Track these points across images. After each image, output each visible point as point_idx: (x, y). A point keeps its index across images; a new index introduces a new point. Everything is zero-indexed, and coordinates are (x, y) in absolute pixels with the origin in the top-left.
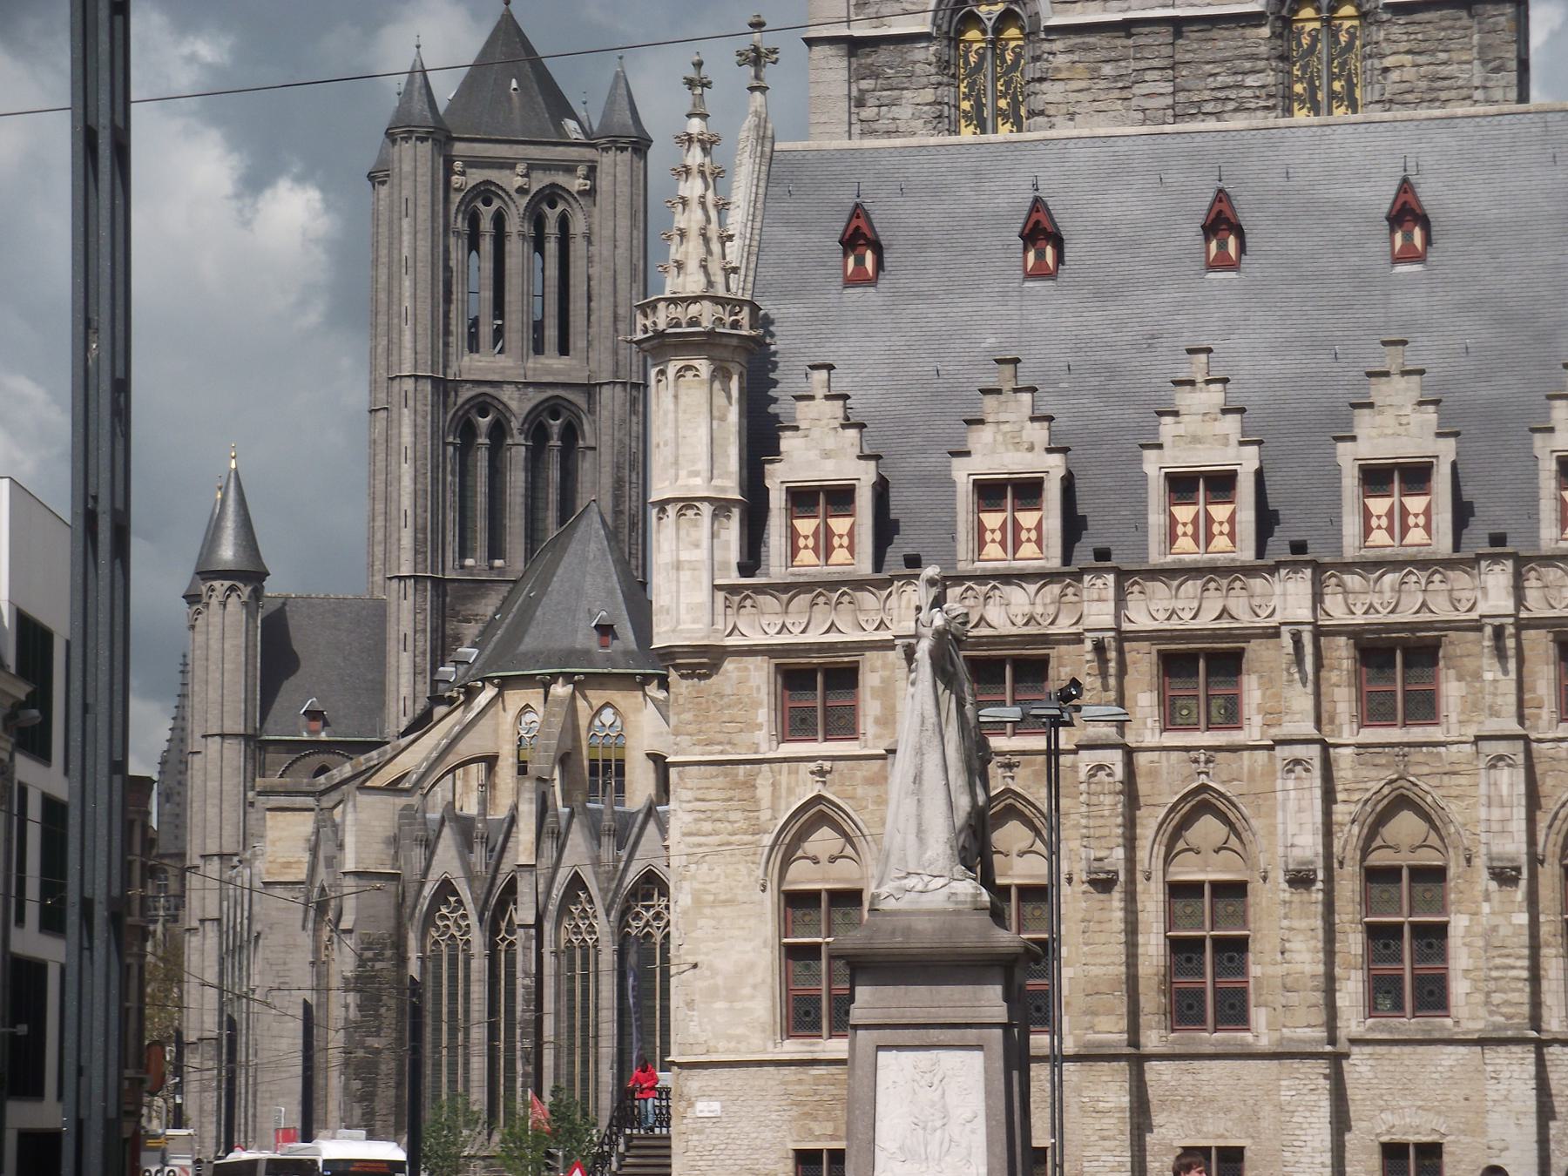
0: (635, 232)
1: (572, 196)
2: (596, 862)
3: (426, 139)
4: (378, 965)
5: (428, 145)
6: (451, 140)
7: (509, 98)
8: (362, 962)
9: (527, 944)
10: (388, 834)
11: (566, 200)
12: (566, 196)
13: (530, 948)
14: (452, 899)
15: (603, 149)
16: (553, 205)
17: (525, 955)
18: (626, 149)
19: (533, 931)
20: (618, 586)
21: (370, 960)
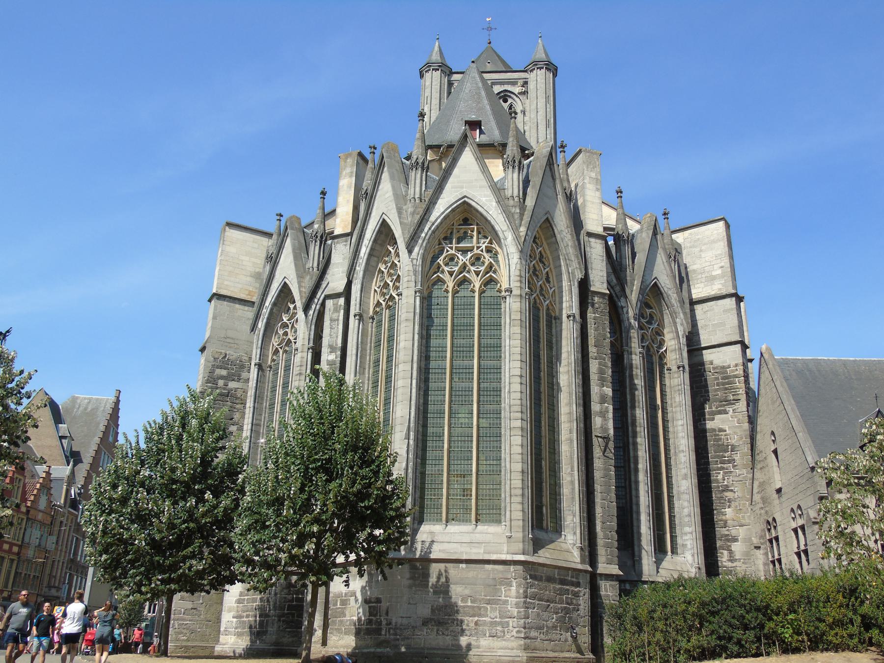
0: (548, 105)
1: (515, 95)
2: (400, 199)
3: (438, 70)
4: (232, 385)
5: (439, 72)
6: (451, 73)
7: (486, 65)
8: (211, 379)
9: (335, 316)
10: (257, 270)
11: (512, 98)
12: (512, 95)
13: (338, 320)
14: (292, 306)
15: (531, 71)
16: (505, 101)
17: (331, 328)
18: (543, 68)
19: (342, 301)
20: (488, 107)
21: (222, 377)
